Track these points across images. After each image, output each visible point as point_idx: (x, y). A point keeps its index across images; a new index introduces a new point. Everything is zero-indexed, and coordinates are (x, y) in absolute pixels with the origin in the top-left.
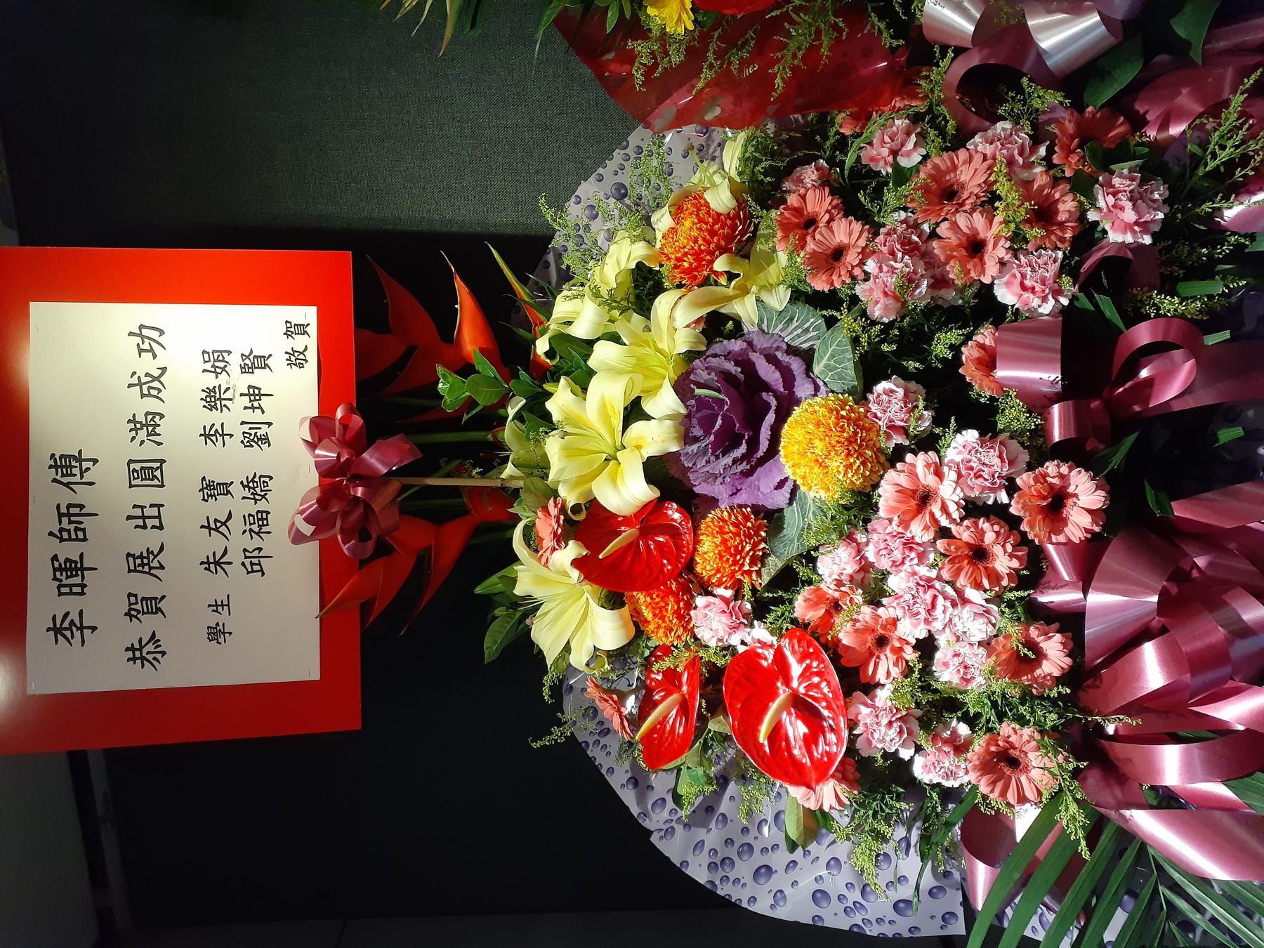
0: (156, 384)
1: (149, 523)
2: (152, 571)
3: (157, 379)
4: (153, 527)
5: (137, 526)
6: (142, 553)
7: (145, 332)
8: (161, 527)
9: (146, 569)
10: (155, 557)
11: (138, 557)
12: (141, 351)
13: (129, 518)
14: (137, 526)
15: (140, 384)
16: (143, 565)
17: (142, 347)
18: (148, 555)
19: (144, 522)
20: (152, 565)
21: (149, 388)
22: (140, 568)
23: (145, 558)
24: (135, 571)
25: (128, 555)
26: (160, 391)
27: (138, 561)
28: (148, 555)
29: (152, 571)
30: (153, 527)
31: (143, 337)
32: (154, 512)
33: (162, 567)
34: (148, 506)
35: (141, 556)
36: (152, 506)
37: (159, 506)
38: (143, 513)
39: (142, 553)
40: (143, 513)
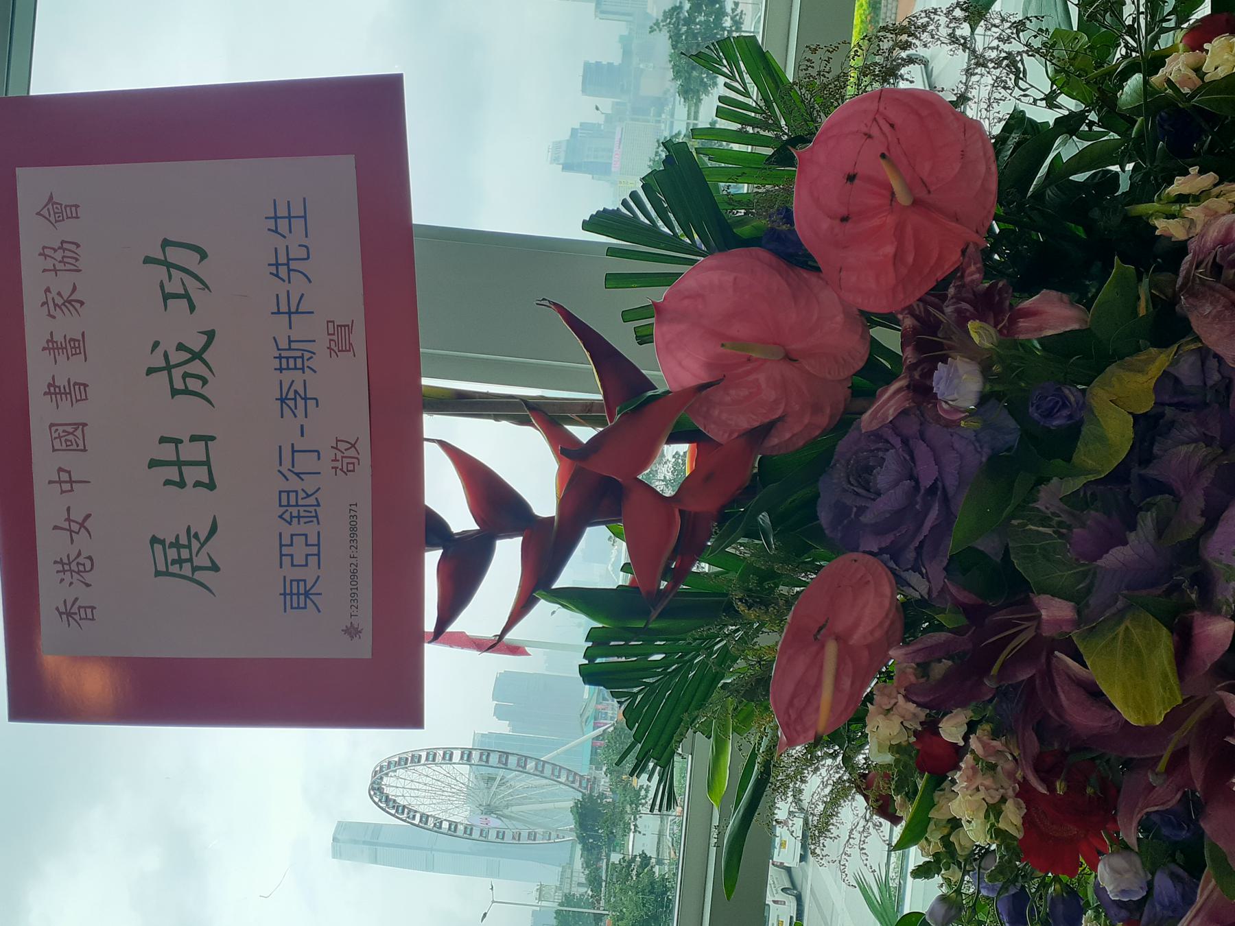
1: (193, 474)
2: (198, 575)
4: (198, 484)
5: (168, 482)
6: (177, 537)
8: (211, 486)
11: (172, 545)
12: (167, 297)
13: (153, 463)
14: (168, 482)
16: (179, 561)
18: (189, 541)
22: (174, 569)
23: (184, 546)
24: (167, 573)
27: (172, 554)
28: (189, 541)
29: (198, 575)
30: (198, 484)
33: (215, 568)
34: (186, 439)
35: (176, 545)
36: (194, 438)
37: (208, 439)
39: (177, 537)
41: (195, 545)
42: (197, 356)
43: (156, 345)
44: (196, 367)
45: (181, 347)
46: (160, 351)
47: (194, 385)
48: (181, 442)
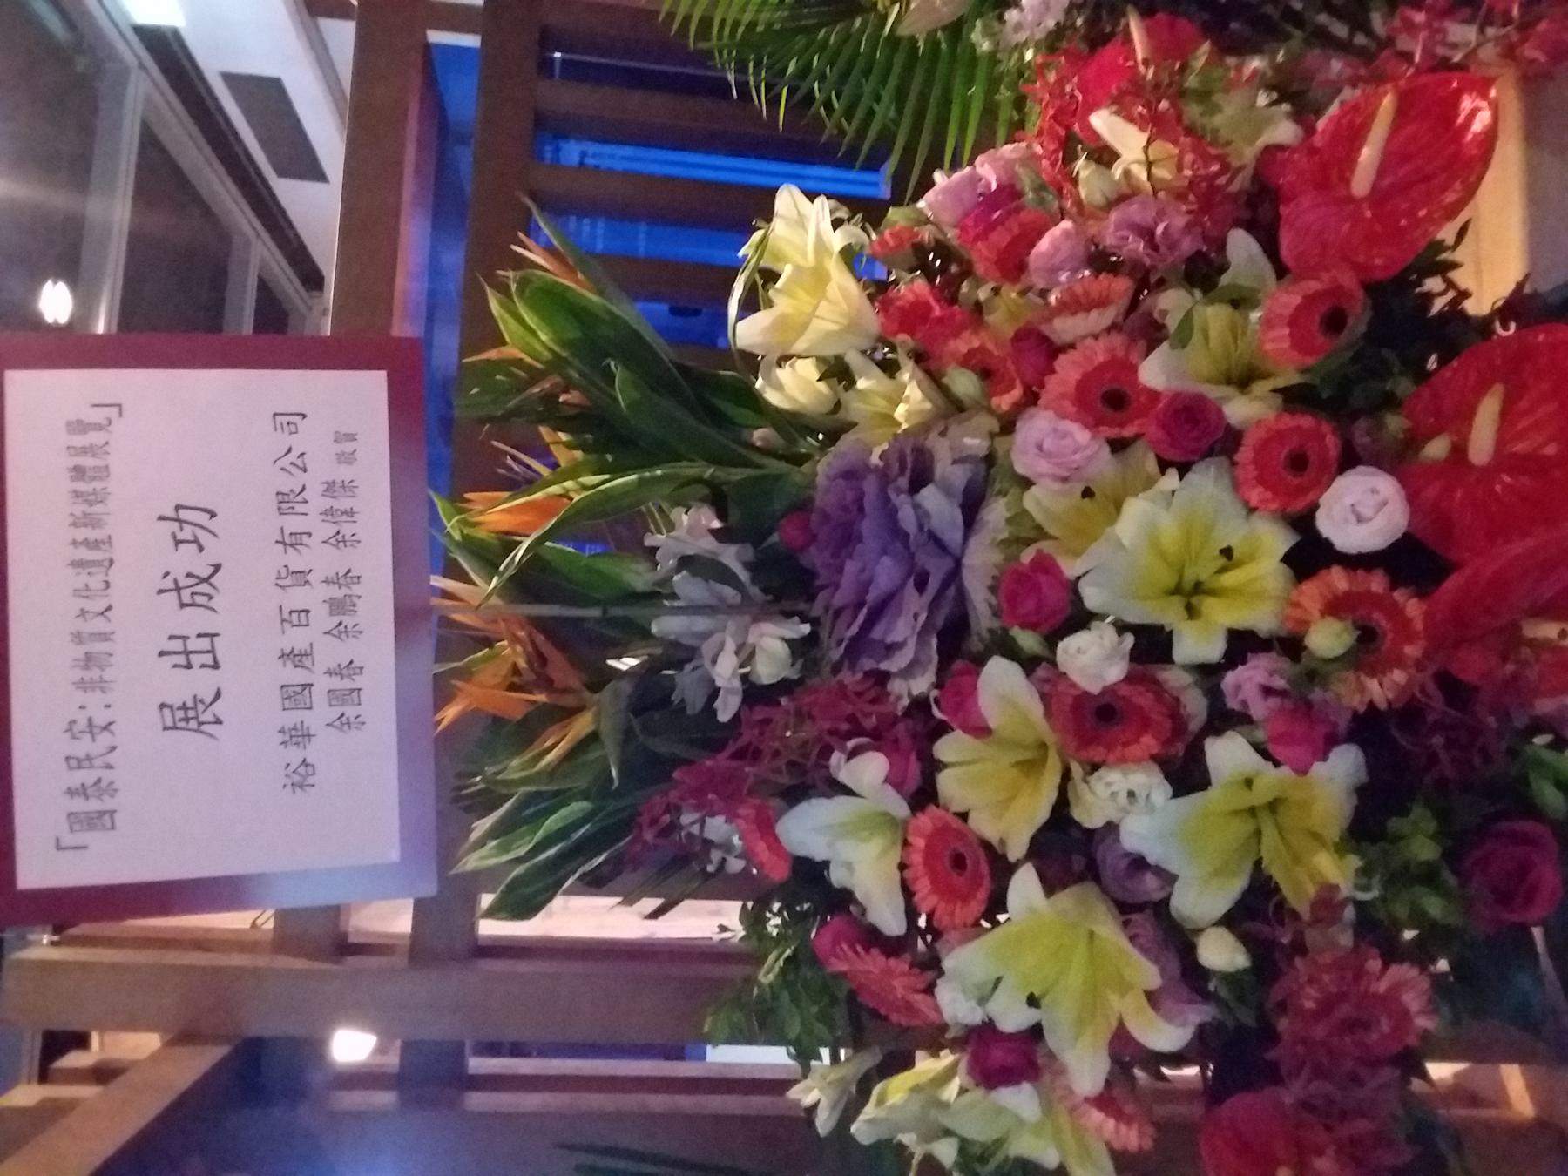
0: (204, 588)
2: (204, 728)
3: (206, 580)
4: (203, 666)
5: (175, 666)
7: (183, 514)
8: (216, 666)
9: (193, 724)
11: (179, 708)
12: (178, 542)
13: (162, 654)
14: (175, 666)
16: (187, 719)
17: (180, 536)
19: (188, 659)
20: (202, 718)
21: (193, 594)
24: (175, 728)
25: (162, 706)
26: (211, 598)
27: (180, 714)
30: (203, 666)
32: (204, 644)
33: (218, 722)
35: (184, 707)
38: (185, 646)
40: (185, 646)
41: (201, 707)
42: (206, 580)
43: (167, 574)
45: (189, 575)
46: (170, 579)
47: (199, 599)
48: (188, 638)
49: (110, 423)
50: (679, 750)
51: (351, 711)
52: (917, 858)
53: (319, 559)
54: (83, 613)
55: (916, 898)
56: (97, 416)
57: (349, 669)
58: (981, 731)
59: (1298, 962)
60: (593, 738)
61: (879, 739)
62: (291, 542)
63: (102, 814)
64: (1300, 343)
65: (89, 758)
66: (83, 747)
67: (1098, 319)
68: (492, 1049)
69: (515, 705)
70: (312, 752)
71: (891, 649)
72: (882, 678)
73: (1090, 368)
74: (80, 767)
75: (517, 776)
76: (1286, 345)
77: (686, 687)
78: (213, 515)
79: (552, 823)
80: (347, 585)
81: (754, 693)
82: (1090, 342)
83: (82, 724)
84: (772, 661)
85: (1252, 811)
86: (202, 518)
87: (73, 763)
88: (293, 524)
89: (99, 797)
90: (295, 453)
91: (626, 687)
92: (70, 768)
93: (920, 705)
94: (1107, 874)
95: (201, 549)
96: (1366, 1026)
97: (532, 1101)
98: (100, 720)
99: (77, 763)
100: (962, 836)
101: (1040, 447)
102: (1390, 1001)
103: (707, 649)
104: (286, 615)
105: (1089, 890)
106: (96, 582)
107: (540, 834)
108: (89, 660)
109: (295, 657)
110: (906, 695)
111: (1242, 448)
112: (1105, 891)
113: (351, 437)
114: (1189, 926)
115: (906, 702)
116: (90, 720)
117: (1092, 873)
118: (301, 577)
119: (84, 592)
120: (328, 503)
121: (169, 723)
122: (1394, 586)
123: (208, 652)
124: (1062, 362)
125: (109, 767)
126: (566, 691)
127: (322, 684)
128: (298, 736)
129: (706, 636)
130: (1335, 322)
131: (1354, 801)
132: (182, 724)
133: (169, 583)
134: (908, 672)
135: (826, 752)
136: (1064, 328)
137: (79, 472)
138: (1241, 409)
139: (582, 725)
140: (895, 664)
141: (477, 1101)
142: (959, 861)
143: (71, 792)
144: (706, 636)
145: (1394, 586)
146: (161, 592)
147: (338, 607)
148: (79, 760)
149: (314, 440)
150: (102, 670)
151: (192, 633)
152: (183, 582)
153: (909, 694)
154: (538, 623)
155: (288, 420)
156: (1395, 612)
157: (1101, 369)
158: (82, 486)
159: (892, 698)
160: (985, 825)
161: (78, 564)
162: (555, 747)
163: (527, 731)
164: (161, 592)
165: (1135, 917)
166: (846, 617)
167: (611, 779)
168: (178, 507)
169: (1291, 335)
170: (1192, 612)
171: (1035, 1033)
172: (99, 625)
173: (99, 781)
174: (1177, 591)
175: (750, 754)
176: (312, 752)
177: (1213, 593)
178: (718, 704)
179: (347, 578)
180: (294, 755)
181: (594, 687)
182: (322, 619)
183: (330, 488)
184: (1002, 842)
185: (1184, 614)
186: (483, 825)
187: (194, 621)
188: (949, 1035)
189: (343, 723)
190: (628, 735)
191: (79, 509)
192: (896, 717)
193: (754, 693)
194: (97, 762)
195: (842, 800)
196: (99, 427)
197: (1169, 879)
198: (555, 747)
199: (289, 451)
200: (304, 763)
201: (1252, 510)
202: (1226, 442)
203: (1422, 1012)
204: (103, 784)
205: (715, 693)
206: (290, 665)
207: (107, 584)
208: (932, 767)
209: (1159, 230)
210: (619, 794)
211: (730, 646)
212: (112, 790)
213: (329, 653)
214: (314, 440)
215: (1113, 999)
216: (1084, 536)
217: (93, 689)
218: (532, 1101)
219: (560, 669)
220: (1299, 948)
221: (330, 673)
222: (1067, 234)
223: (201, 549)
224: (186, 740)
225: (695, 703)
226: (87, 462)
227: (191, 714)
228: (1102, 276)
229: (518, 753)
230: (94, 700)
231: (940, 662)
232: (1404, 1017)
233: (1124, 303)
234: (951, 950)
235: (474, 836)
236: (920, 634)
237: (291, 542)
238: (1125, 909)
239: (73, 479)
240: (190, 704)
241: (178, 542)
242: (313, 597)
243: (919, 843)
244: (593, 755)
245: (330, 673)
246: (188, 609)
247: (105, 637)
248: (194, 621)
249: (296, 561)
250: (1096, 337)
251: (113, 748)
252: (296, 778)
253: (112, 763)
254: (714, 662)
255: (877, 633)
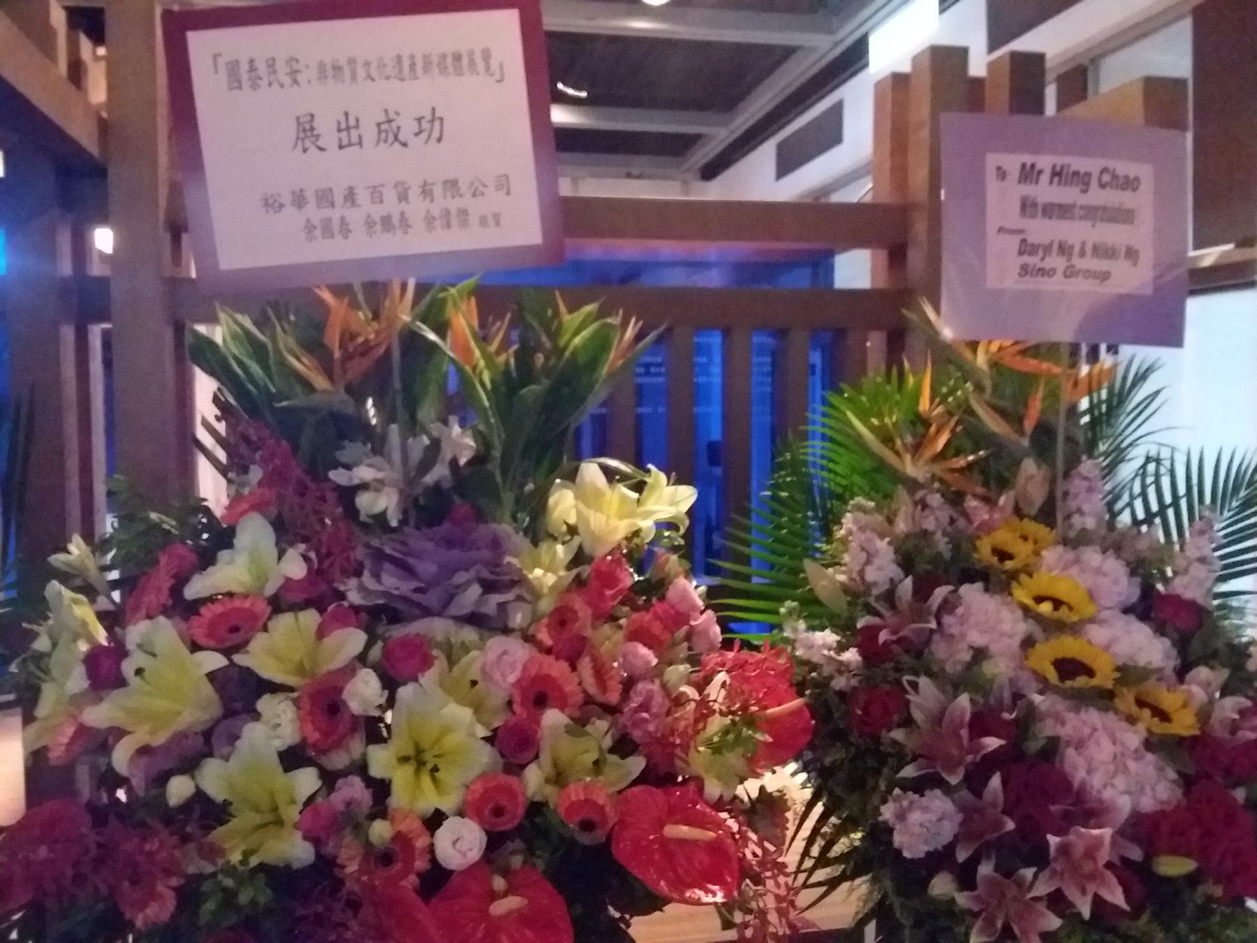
2: (300, 143)
4: (340, 140)
8: (341, 147)
9: (302, 135)
10: (314, 143)
12: (419, 120)
13: (346, 114)
14: (339, 123)
15: (389, 121)
16: (305, 131)
17: (423, 122)
25: (312, 116)
30: (340, 140)
31: (432, 121)
33: (305, 150)
35: (312, 129)
36: (360, 137)
37: (360, 143)
41: (313, 139)
42: (396, 138)
44: (391, 138)
45: (399, 128)
47: (383, 135)
49: (492, 75)
50: (305, 443)
51: (318, 233)
52: (237, 603)
53: (417, 207)
54: (367, 64)
55: (209, 604)
56: (494, 66)
57: (345, 230)
58: (321, 633)
59: (175, 839)
60: (309, 387)
61: (317, 574)
62: (426, 191)
63: (239, 82)
64: (573, 808)
65: (275, 72)
66: (281, 67)
67: (590, 684)
68: (107, 346)
69: (333, 339)
70: (289, 211)
71: (377, 576)
72: (358, 573)
73: (560, 682)
74: (269, 66)
75: (281, 345)
76: (574, 799)
77: (351, 450)
78: (439, 140)
79: (255, 368)
80: (401, 226)
81: (348, 495)
82: (576, 680)
83: (295, 66)
84: (367, 503)
85: (275, 809)
86: (436, 134)
87: (271, 63)
88: (438, 191)
89: (250, 79)
90: (481, 188)
91: (350, 408)
92: (267, 61)
93: (342, 596)
94: (227, 722)
95: (417, 134)
96: (134, 883)
97: (69, 370)
98: (300, 77)
99: (271, 64)
100: (253, 630)
101: (505, 653)
102: (152, 896)
103: (378, 460)
104: (377, 189)
105: (216, 710)
106: (389, 70)
107: (246, 360)
108: (337, 69)
109: (350, 197)
110: (347, 588)
111: (505, 776)
112: (217, 722)
113: (498, 223)
114: (196, 773)
115: (342, 588)
116: (299, 71)
117: (229, 713)
118: (403, 197)
119: (382, 65)
120: (454, 212)
121: (302, 120)
122: (419, 875)
123: (350, 140)
124: (564, 666)
125: (270, 85)
126: (345, 371)
127: (335, 214)
128: (299, 200)
129: (390, 461)
130: (587, 826)
131: (281, 865)
132: (301, 129)
133: (392, 116)
134: (362, 588)
135: (305, 540)
136: (585, 665)
137: (457, 57)
138: (534, 779)
139: (320, 382)
140: (367, 578)
141: (68, 333)
142: (235, 629)
143: (252, 61)
144: (390, 461)
145: (419, 875)
146: (386, 111)
147: (386, 222)
148: (273, 66)
149: (493, 201)
150: (333, 77)
151: (361, 131)
152: (394, 125)
153: (347, 591)
154: (388, 352)
155: (504, 184)
156: (404, 875)
157: (560, 690)
158: (449, 59)
159: (345, 580)
160: (259, 642)
161: (399, 59)
162: (302, 365)
163: (314, 346)
164: (386, 111)
165: (201, 739)
166: (399, 547)
167: (281, 401)
168: (441, 119)
169: (580, 801)
170: (404, 760)
171: (121, 682)
172: (361, 73)
173: (261, 79)
174: (419, 751)
175: (302, 491)
176: (289, 211)
177: (418, 771)
178: (341, 471)
179: (405, 224)
180: (286, 199)
181: (349, 389)
182: (378, 212)
183: (463, 213)
184: (247, 652)
185: (403, 753)
186: (247, 323)
187: (369, 133)
188: (117, 629)
189: (310, 228)
190: (313, 411)
191: (435, 59)
192: (333, 581)
193: (348, 495)
194: (272, 77)
195: (274, 553)
196: (488, 68)
197: (226, 758)
198: (302, 365)
199: (486, 186)
200: (282, 206)
201: (467, 787)
202: (515, 768)
203: (146, 917)
204: (259, 82)
205: (348, 467)
206: (346, 193)
207: (388, 78)
208: (295, 608)
209: (645, 715)
210: (272, 407)
211: (380, 475)
212: (255, 86)
213: (355, 217)
214: (493, 201)
215: (147, 728)
216: (449, 689)
217: (320, 72)
218: (69, 370)
219: (359, 367)
220: (185, 839)
221: (342, 219)
222: (649, 662)
223: (417, 134)
224: (291, 132)
225: (344, 456)
226: (465, 61)
227: (309, 134)
228: (621, 686)
229: (298, 343)
230: (313, 73)
231: (368, 607)
232: (142, 906)
233: (600, 698)
234: (174, 626)
235: (239, 317)
236: (388, 592)
237: (426, 191)
238: (207, 735)
239: (454, 54)
240: (315, 133)
241: (419, 120)
242: (391, 205)
243: (247, 604)
244: (298, 389)
245: (342, 219)
246: (376, 129)
247: (354, 77)
248: (369, 133)
249: (414, 194)
250: (580, 684)
251: (282, 86)
252: (271, 201)
253: (273, 86)
254: (369, 466)
255: (387, 566)
